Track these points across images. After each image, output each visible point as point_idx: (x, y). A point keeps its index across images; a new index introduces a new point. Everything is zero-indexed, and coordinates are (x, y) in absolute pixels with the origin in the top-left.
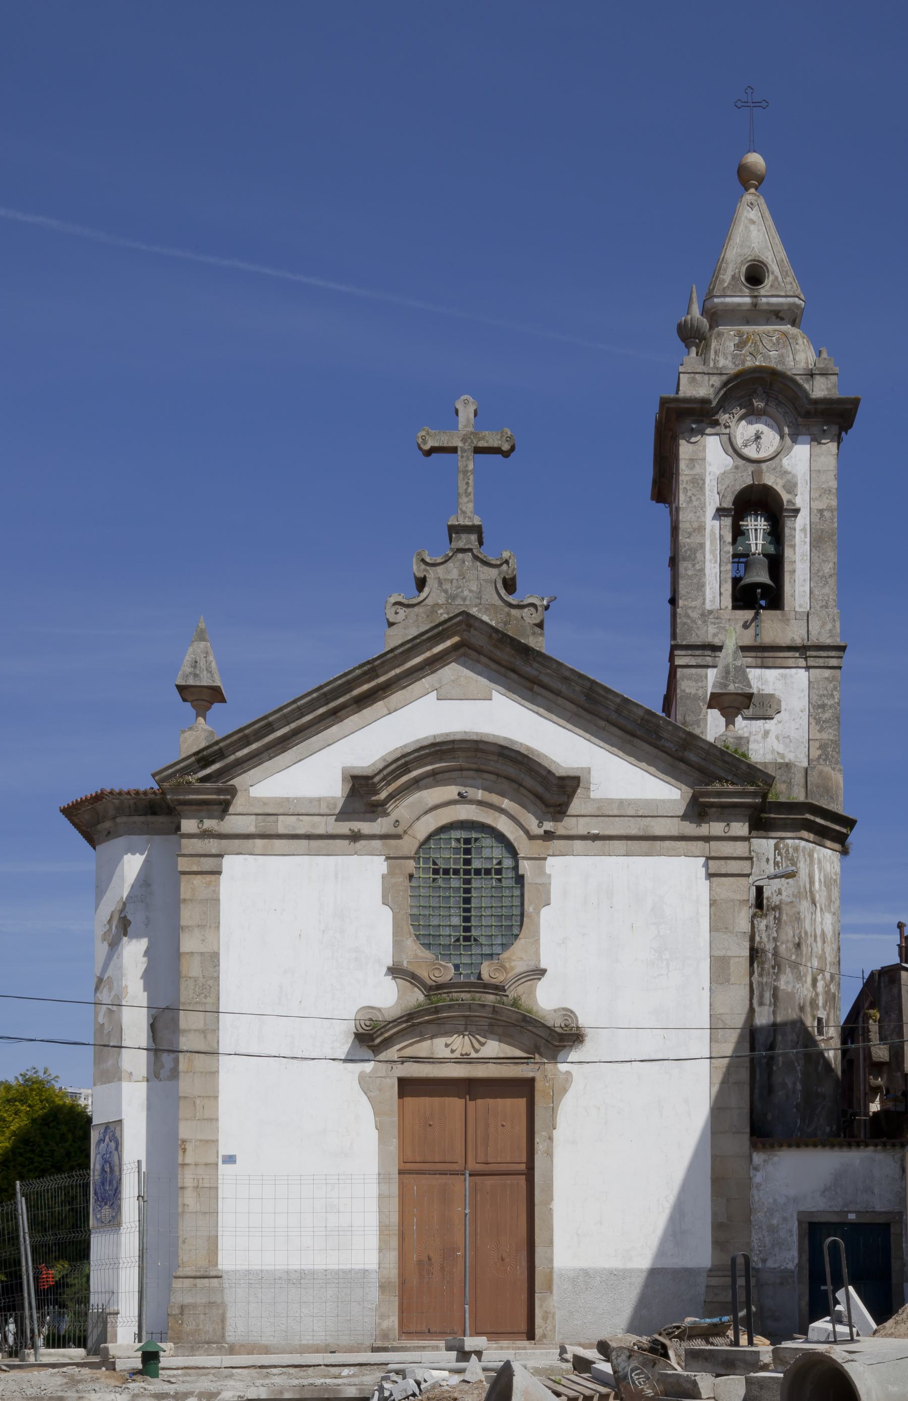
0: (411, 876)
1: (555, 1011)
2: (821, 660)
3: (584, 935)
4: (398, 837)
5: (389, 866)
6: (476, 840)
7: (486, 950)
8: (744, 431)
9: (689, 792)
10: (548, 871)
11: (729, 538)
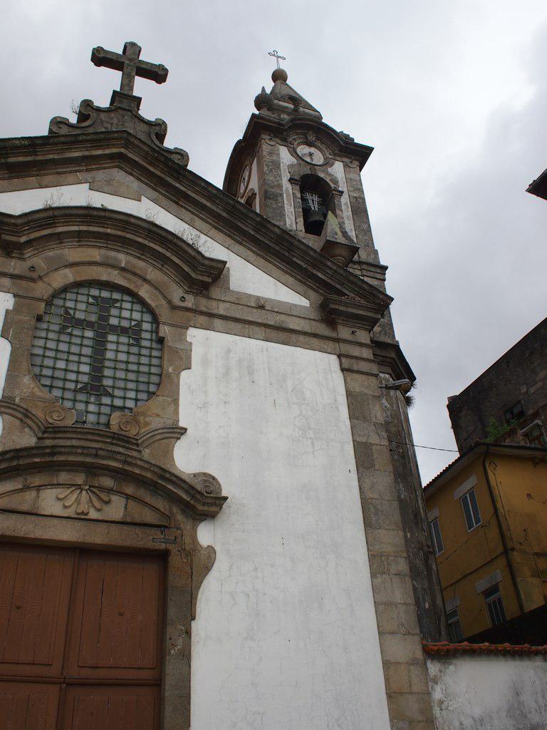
0: (39, 319)
1: (195, 475)
2: (372, 273)
3: (226, 402)
4: (33, 280)
5: (16, 304)
6: (117, 301)
7: (118, 403)
8: (303, 150)
9: (317, 298)
10: (188, 340)
11: (299, 195)
